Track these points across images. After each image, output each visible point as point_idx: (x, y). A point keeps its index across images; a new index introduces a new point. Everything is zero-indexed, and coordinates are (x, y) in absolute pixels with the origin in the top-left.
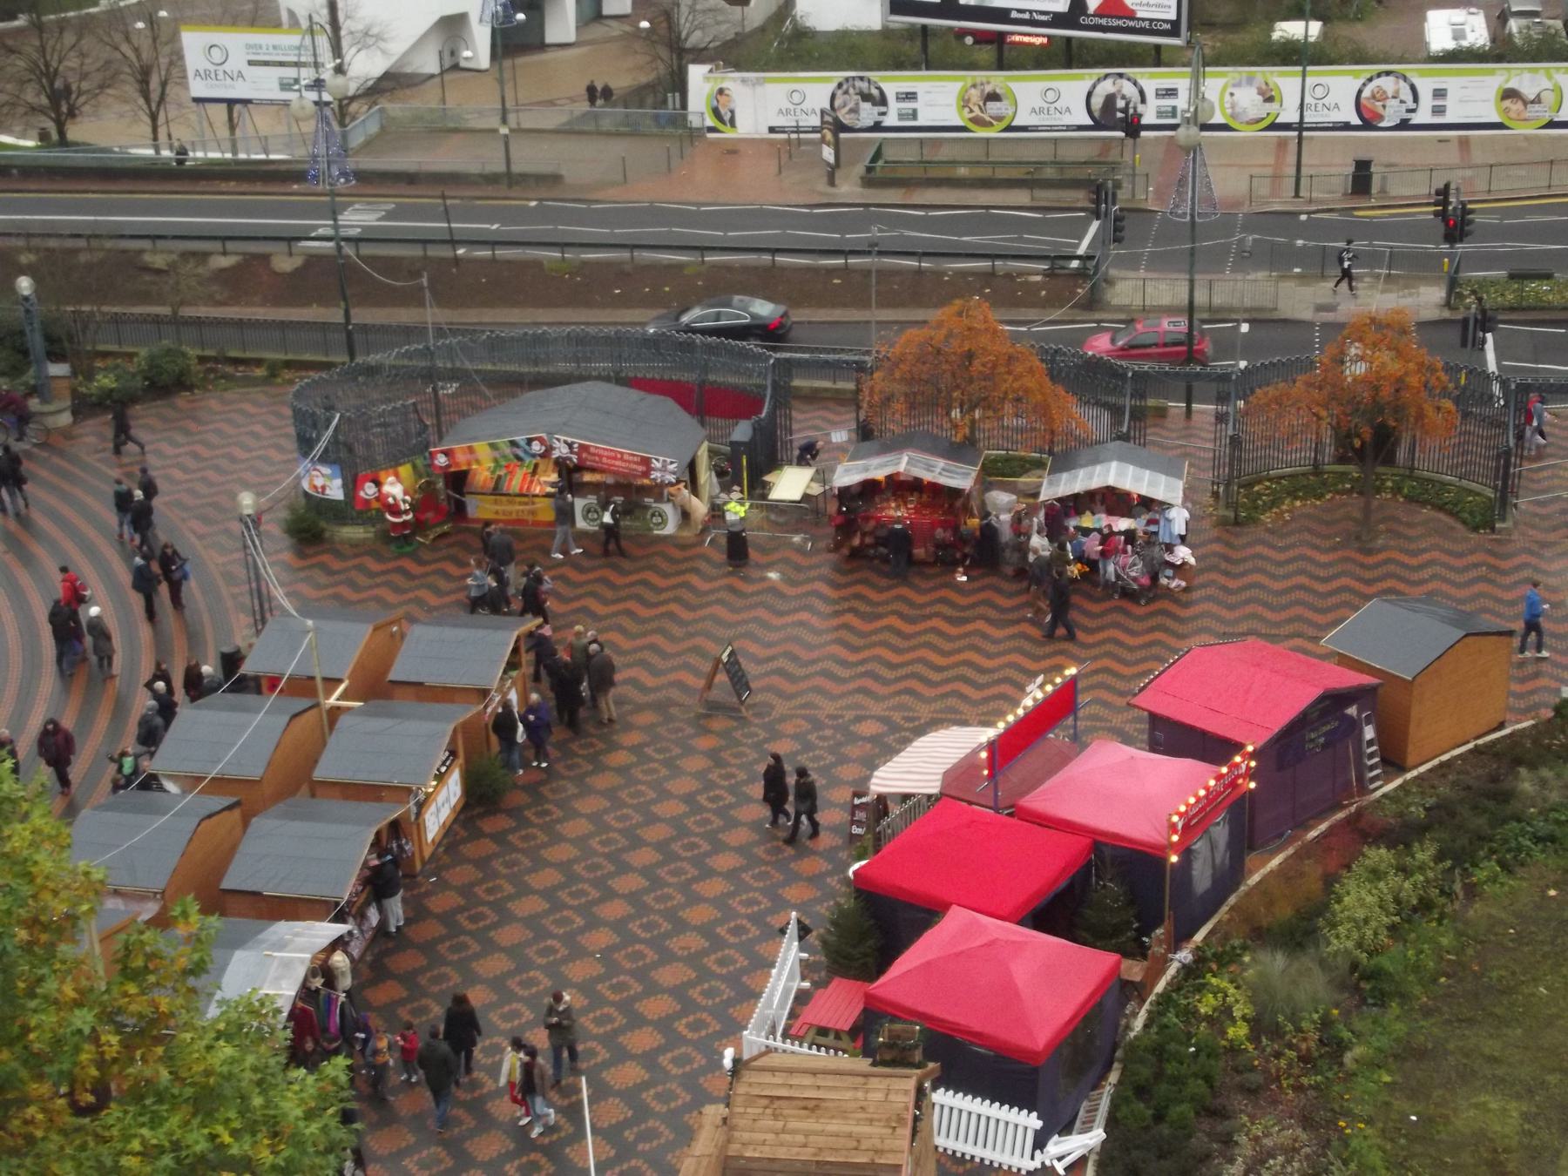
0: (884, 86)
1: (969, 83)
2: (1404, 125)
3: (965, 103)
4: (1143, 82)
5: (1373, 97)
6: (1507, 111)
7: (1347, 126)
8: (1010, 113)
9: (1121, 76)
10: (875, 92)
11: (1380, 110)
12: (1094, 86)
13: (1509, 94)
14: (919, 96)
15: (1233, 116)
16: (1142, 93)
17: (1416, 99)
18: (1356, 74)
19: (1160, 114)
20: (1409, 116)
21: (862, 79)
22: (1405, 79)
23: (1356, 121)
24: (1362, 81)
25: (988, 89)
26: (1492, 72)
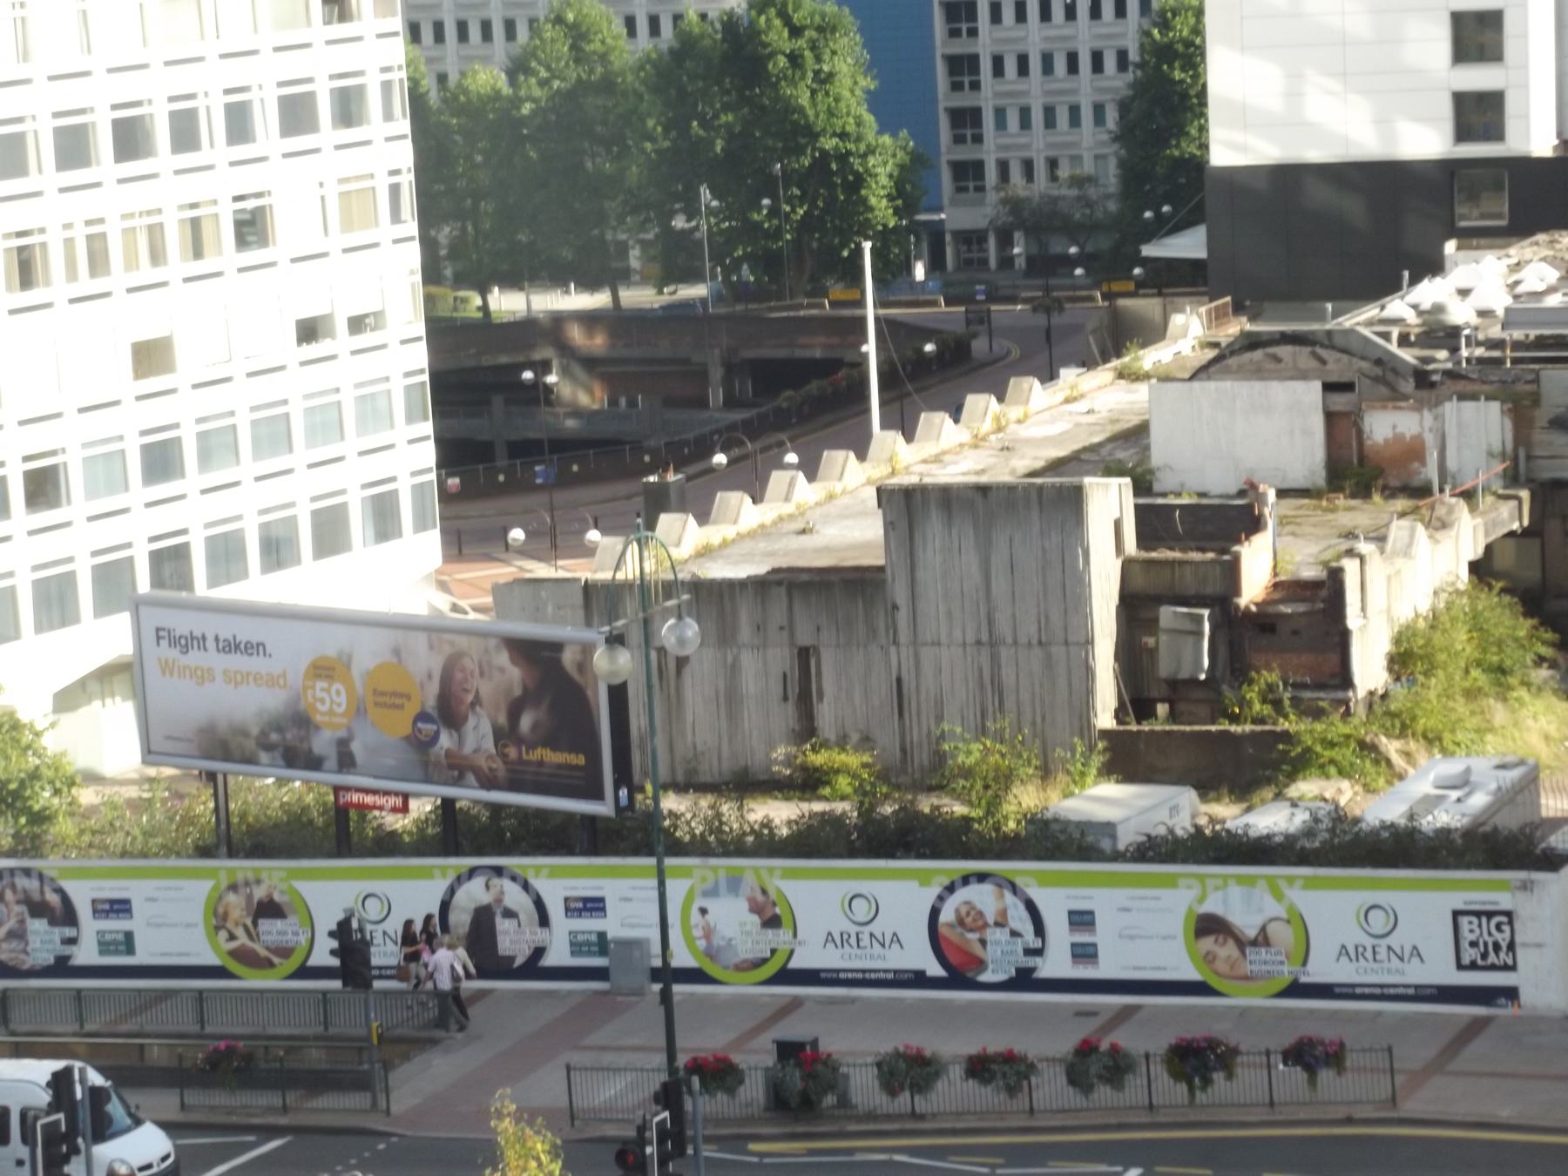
0: (69, 886)
1: (224, 884)
2: (1024, 980)
3: (218, 920)
4: (541, 885)
5: (961, 922)
6: (1209, 959)
7: (918, 979)
8: (303, 939)
9: (498, 871)
10: (53, 898)
11: (977, 949)
12: (452, 891)
13: (1209, 926)
14: (136, 906)
15: (711, 954)
16: (539, 904)
17: (1040, 929)
18: (924, 879)
19: (577, 947)
20: (1031, 962)
21: (27, 872)
22: (1014, 889)
23: (935, 969)
24: (935, 891)
25: (259, 893)
26: (1171, 882)
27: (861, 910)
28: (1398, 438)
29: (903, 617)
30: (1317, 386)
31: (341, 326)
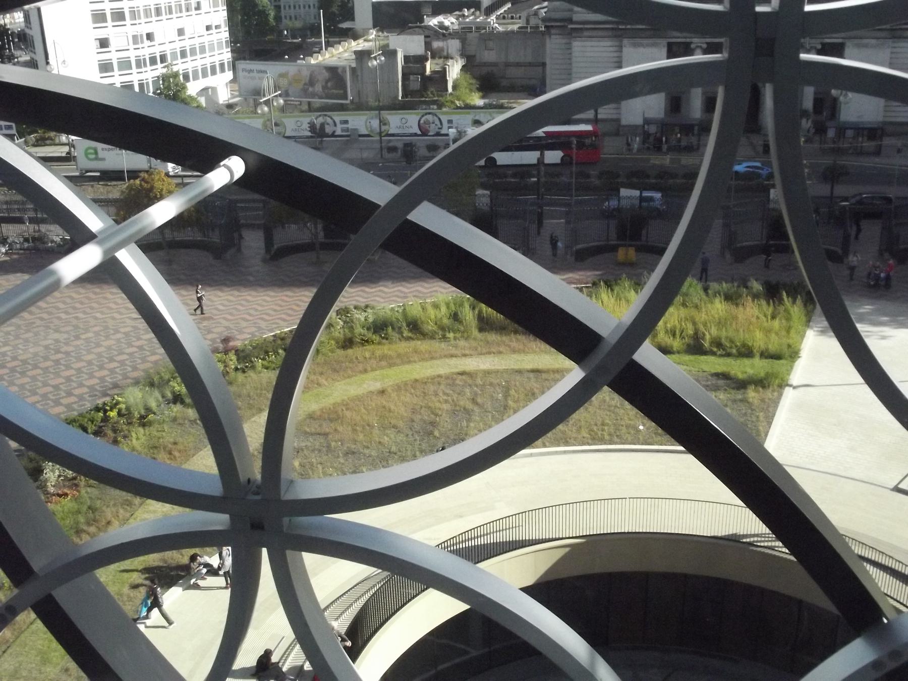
1: (266, 119)
2: (438, 134)
4: (335, 118)
5: (425, 122)
7: (416, 135)
8: (283, 131)
9: (326, 115)
11: (428, 128)
16: (334, 122)
19: (343, 130)
20: (439, 130)
22: (436, 116)
23: (419, 132)
24: (420, 116)
26: (469, 113)
27: (404, 121)
28: (439, 47)
29: (359, 78)
30: (423, 37)
31: (214, 27)
